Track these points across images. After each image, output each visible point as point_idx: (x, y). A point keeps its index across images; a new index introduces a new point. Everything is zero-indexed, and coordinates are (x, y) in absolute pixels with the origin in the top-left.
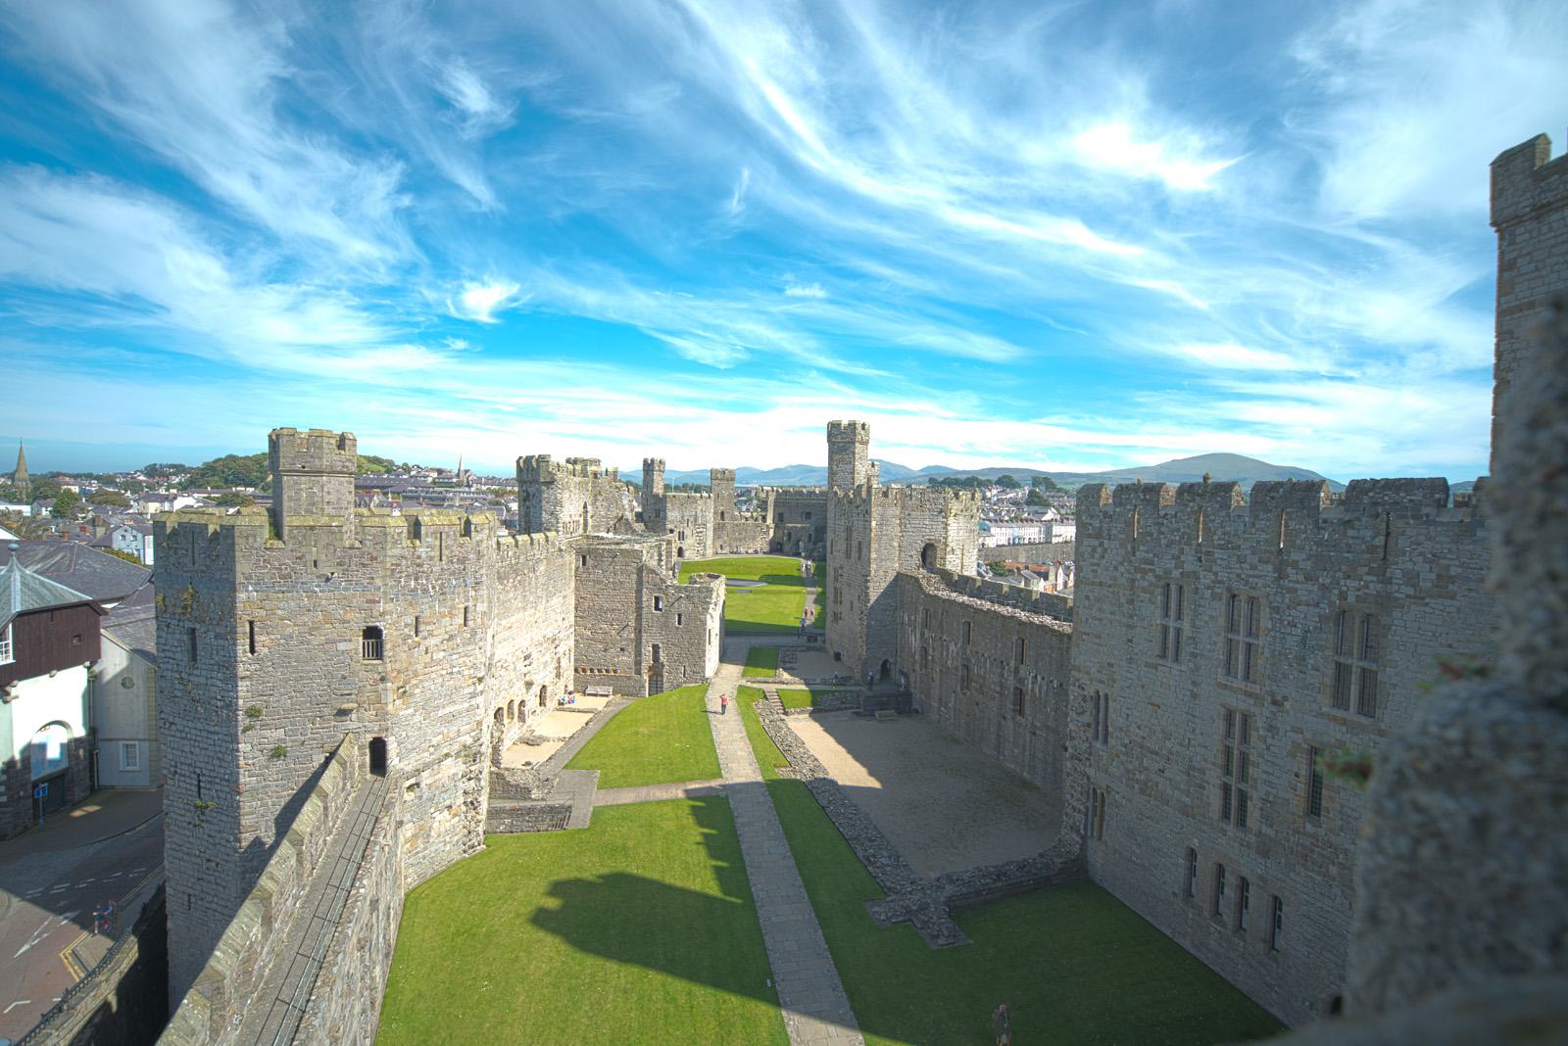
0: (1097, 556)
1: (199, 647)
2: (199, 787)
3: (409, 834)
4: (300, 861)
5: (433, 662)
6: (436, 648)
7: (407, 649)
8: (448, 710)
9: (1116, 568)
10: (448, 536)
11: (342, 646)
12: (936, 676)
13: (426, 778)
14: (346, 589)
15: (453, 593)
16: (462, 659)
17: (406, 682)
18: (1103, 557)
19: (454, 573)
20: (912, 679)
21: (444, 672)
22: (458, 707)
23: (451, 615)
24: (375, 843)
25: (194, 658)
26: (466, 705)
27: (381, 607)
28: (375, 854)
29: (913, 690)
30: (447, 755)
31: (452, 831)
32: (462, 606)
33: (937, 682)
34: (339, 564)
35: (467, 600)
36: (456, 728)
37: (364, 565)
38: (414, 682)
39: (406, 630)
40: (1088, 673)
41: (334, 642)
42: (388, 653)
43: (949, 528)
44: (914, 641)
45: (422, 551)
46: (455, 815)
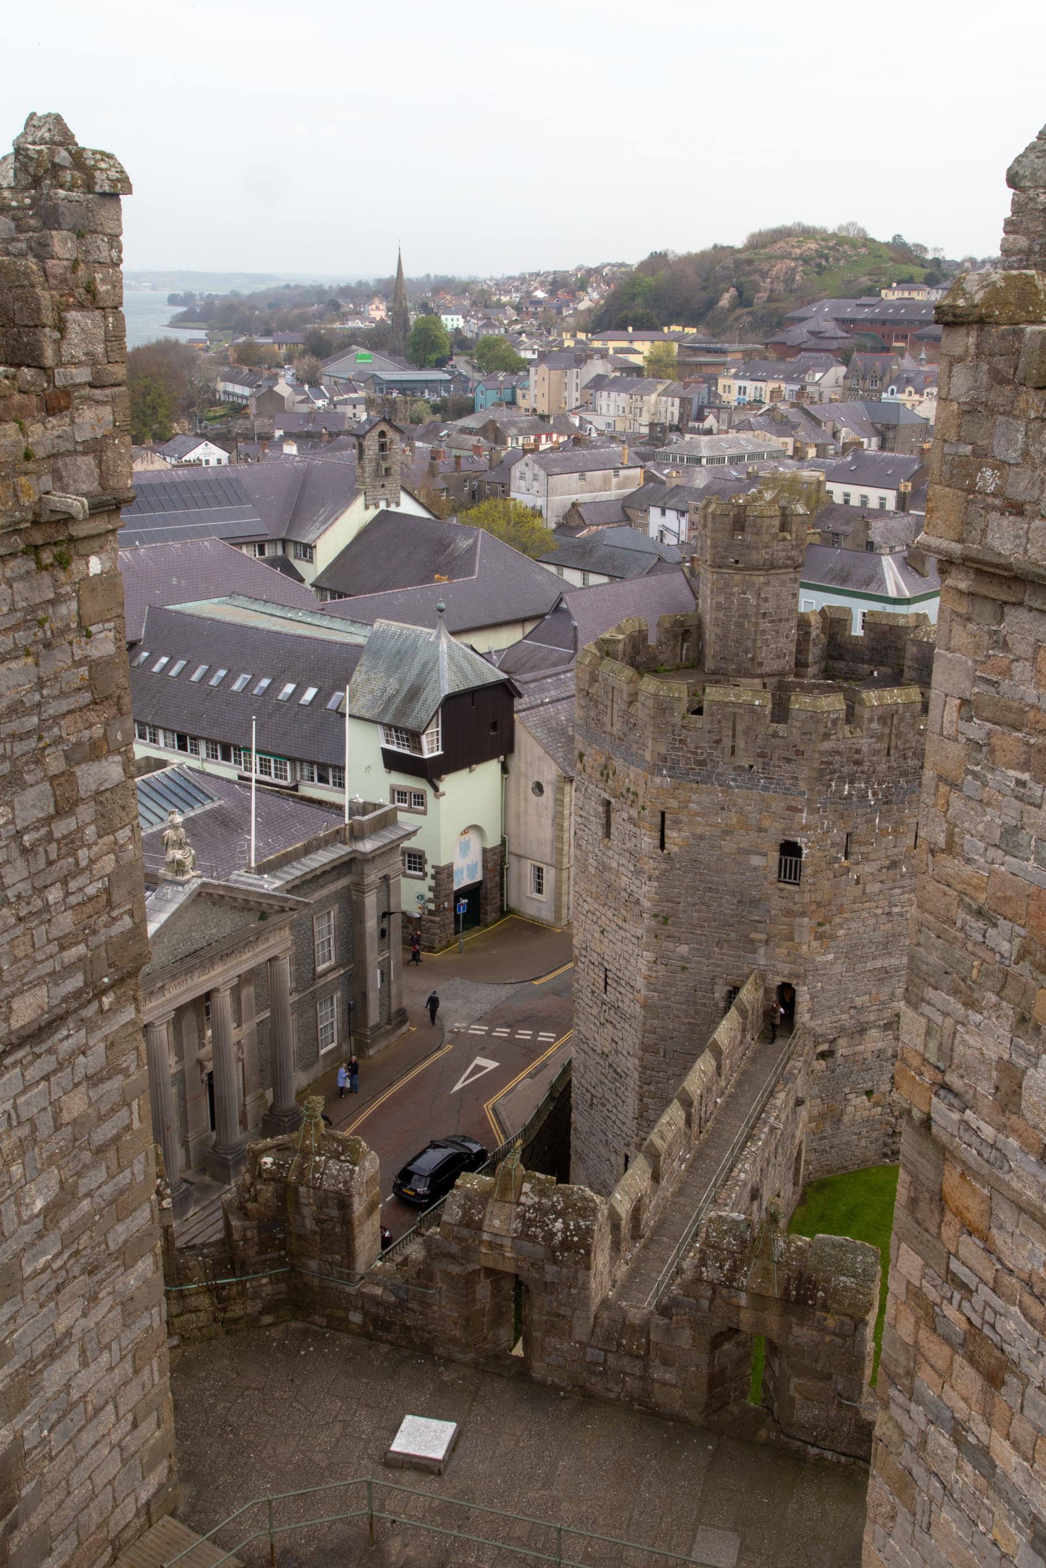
1: (613, 826)
2: (606, 983)
4: (688, 1122)
5: (865, 897)
6: (871, 878)
7: (831, 876)
8: (879, 963)
11: (756, 860)
13: (842, 1048)
14: (765, 788)
15: (902, 802)
16: (906, 896)
21: (879, 911)
24: (765, 1123)
25: (608, 835)
27: (804, 818)
28: (763, 1136)
34: (762, 755)
36: (888, 990)
37: (789, 761)
39: (833, 851)
41: (747, 852)
46: (877, 1104)
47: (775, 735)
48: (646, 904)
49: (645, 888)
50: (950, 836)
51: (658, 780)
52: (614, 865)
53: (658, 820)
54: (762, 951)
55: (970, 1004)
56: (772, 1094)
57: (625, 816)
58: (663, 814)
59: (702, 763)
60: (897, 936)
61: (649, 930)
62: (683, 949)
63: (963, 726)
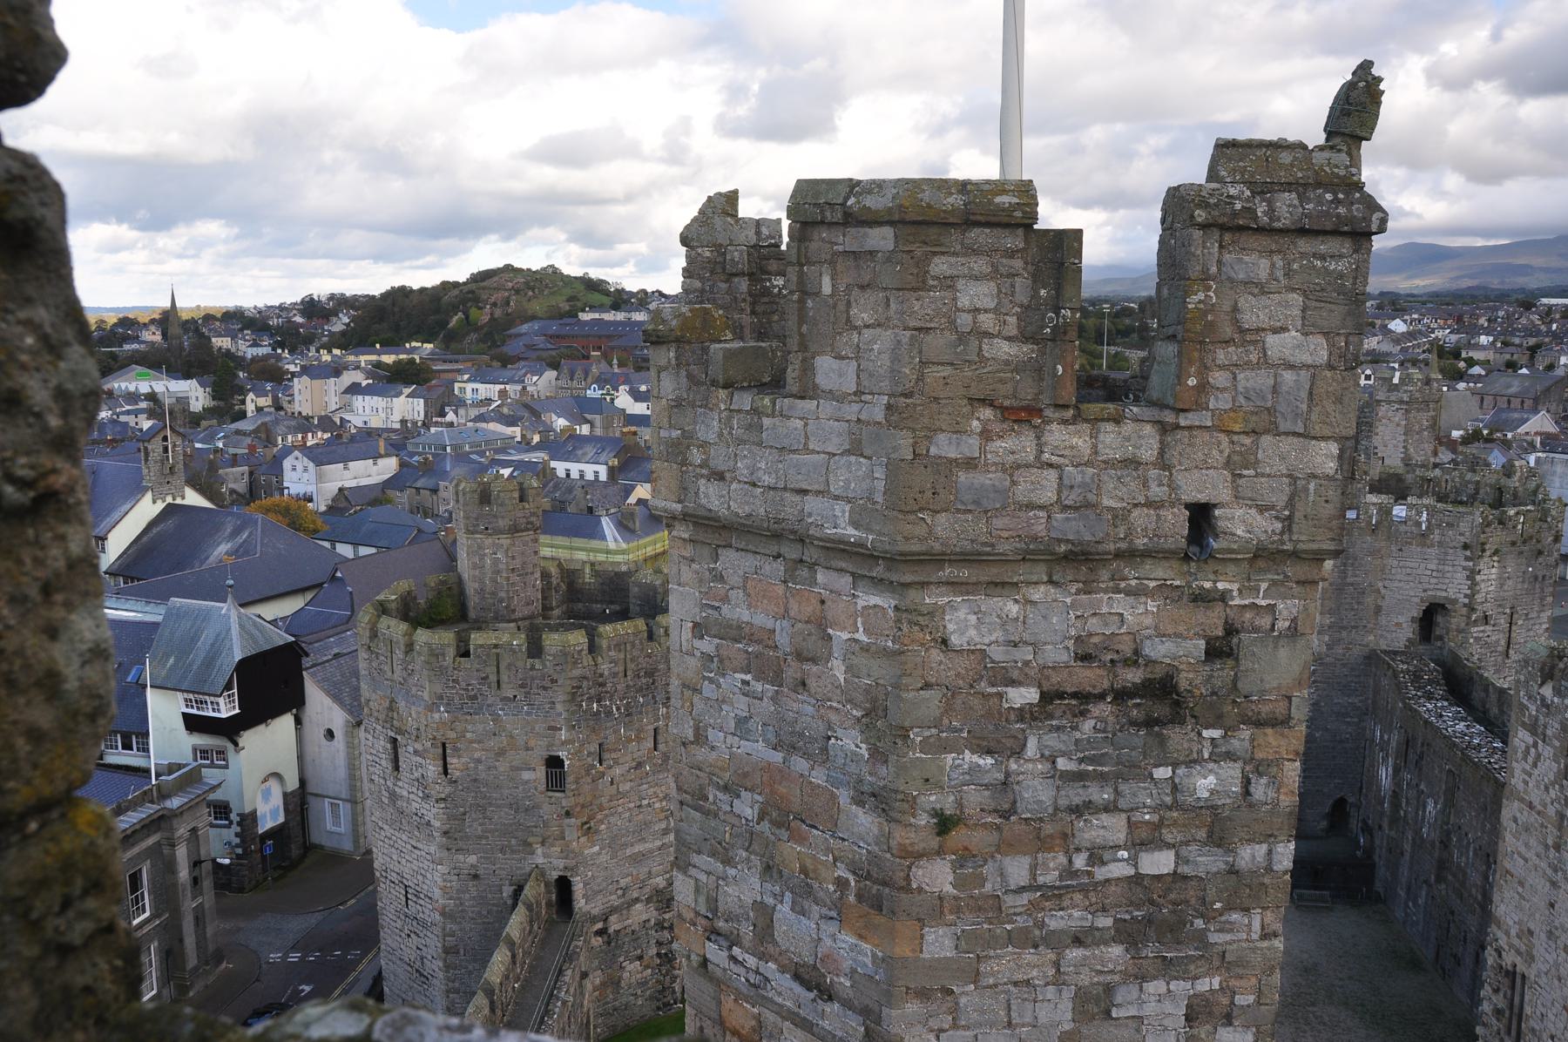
0: (1530, 760)
1: (401, 759)
3: (598, 981)
4: (492, 1010)
5: (620, 795)
8: (638, 848)
9: (1547, 789)
10: (633, 646)
11: (526, 775)
12: (1407, 847)
14: (528, 714)
17: (591, 818)
18: (1535, 765)
19: (641, 690)
20: (1377, 842)
22: (649, 846)
23: (639, 739)
25: (397, 768)
26: (658, 843)
27: (563, 735)
29: (1376, 858)
30: (637, 900)
31: (643, 984)
32: (651, 727)
33: (1407, 856)
34: (522, 686)
35: (658, 720)
37: (545, 688)
38: (599, 817)
40: (1507, 934)
41: (519, 769)
42: (570, 783)
43: (1478, 578)
44: (1385, 775)
45: (605, 668)
46: (647, 967)
47: (533, 668)
48: (437, 824)
49: (434, 811)
50: (697, 729)
51: (437, 716)
52: (405, 793)
53: (440, 751)
54: (539, 851)
55: (728, 861)
56: (561, 972)
57: (411, 749)
58: (444, 745)
59: (474, 698)
60: (647, 824)
61: (441, 847)
62: (472, 859)
63: (697, 643)
